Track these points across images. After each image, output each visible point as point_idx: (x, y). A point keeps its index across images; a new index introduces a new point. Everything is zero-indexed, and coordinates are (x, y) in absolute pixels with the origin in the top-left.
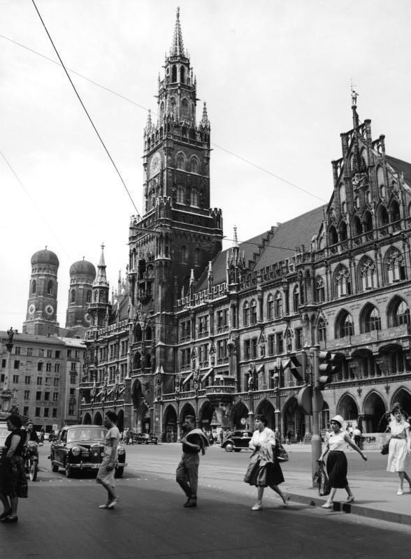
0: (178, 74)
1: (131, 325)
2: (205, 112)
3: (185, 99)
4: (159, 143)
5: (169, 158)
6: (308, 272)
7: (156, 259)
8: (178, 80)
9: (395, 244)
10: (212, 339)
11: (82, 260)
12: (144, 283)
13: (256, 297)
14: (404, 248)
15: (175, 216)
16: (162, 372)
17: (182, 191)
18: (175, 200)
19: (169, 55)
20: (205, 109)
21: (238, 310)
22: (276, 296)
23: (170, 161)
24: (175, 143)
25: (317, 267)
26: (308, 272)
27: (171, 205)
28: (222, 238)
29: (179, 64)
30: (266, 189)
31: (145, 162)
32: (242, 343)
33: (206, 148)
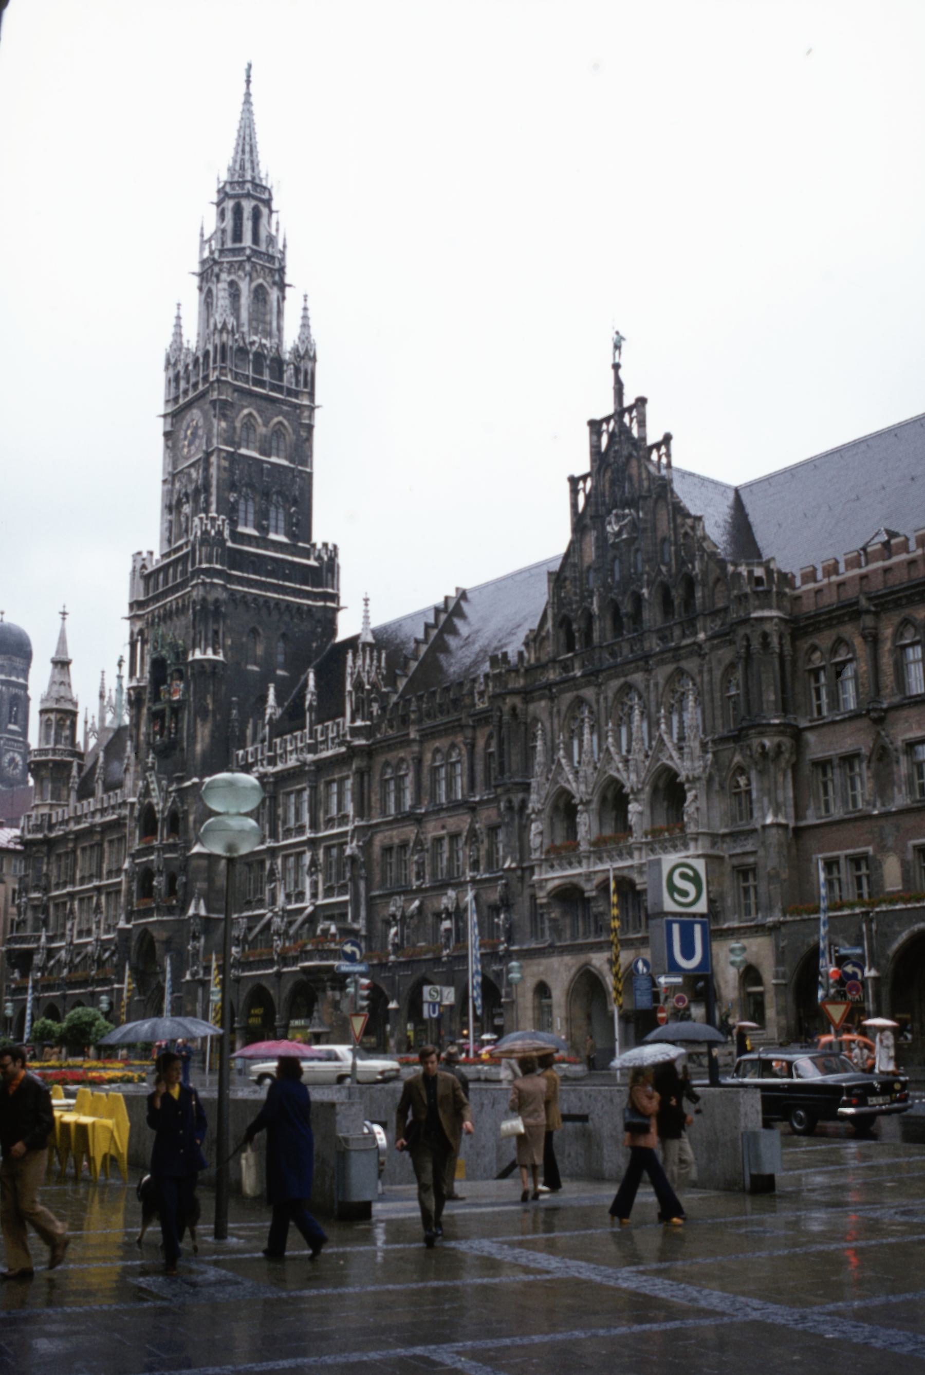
0: (248, 226)
1: (133, 804)
3: (261, 286)
4: (201, 387)
5: (223, 424)
6: (514, 709)
7: (190, 658)
8: (247, 241)
9: (684, 664)
10: (313, 843)
12: (163, 711)
14: (701, 672)
15: (236, 559)
16: (203, 912)
17: (250, 503)
18: (234, 523)
19: (225, 176)
21: (369, 781)
23: (225, 431)
24: (237, 389)
25: (533, 700)
26: (514, 709)
27: (226, 533)
28: (337, 610)
29: (245, 201)
30: (439, 516)
31: (169, 428)
32: (377, 850)
33: (306, 402)
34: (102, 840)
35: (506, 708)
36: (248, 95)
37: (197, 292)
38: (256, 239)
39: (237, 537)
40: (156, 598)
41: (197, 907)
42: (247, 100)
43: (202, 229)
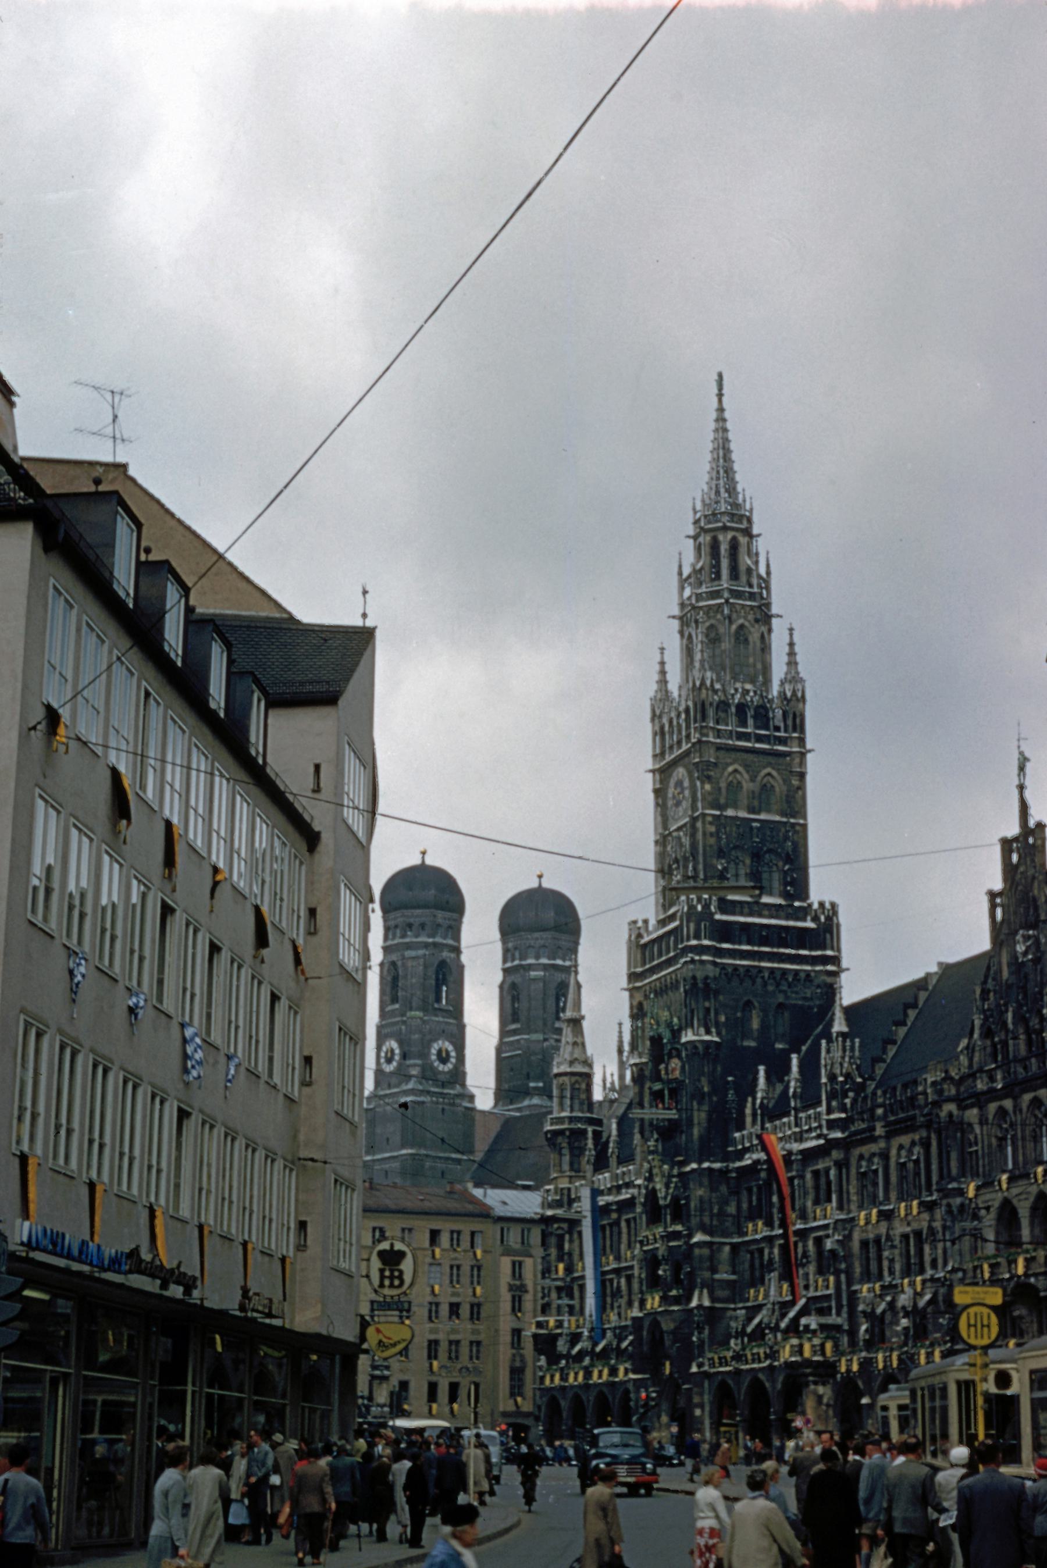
0: (725, 563)
1: (639, 1186)
2: (792, 654)
5: (708, 787)
6: (950, 1115)
7: (684, 1040)
11: (534, 884)
12: (661, 1091)
13: (874, 1148)
15: (725, 932)
16: (707, 1303)
20: (791, 645)
22: (910, 1152)
23: (709, 793)
24: (719, 748)
28: (835, 974)
31: (658, 786)
32: (856, 1245)
34: (619, 1219)
35: (943, 1114)
36: (721, 410)
37: (678, 636)
38: (734, 574)
39: (725, 906)
40: (653, 970)
41: (700, 1298)
42: (721, 419)
43: (680, 567)
